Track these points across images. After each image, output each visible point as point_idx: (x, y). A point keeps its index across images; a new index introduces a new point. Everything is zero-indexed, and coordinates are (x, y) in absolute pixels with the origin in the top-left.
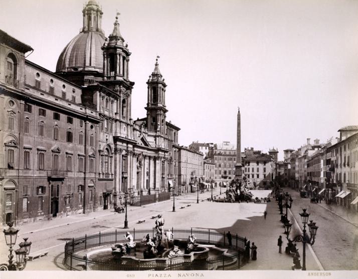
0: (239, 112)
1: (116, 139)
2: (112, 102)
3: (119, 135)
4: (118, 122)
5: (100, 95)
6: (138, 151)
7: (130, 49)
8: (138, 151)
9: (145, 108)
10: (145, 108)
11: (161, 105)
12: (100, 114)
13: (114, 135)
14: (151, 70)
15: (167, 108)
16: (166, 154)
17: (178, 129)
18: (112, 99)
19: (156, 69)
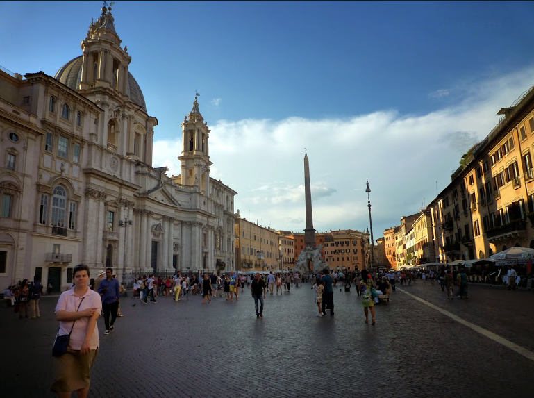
1: (89, 173)
2: (81, 115)
3: (95, 166)
5: (46, 92)
7: (130, 53)
8: (149, 206)
9: (180, 158)
10: (180, 158)
12: (44, 122)
13: (84, 165)
14: (189, 109)
15: (210, 160)
16: (210, 220)
17: (234, 193)
18: (81, 108)
19: (196, 105)
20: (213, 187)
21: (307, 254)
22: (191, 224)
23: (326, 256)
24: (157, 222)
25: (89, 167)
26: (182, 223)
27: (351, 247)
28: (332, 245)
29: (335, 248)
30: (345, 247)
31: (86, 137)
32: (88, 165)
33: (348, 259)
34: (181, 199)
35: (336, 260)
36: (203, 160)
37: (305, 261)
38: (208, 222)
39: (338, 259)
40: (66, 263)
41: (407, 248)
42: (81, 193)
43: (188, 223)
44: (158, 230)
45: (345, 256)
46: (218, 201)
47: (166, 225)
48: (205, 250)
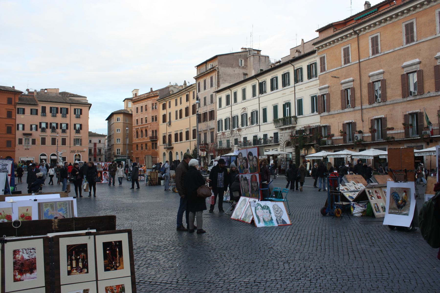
23: (19, 134)
27: (71, 119)
28: (34, 112)
29: (37, 119)
30: (59, 119)
33: (64, 142)
35: (38, 142)
39: (43, 141)
45: (59, 135)
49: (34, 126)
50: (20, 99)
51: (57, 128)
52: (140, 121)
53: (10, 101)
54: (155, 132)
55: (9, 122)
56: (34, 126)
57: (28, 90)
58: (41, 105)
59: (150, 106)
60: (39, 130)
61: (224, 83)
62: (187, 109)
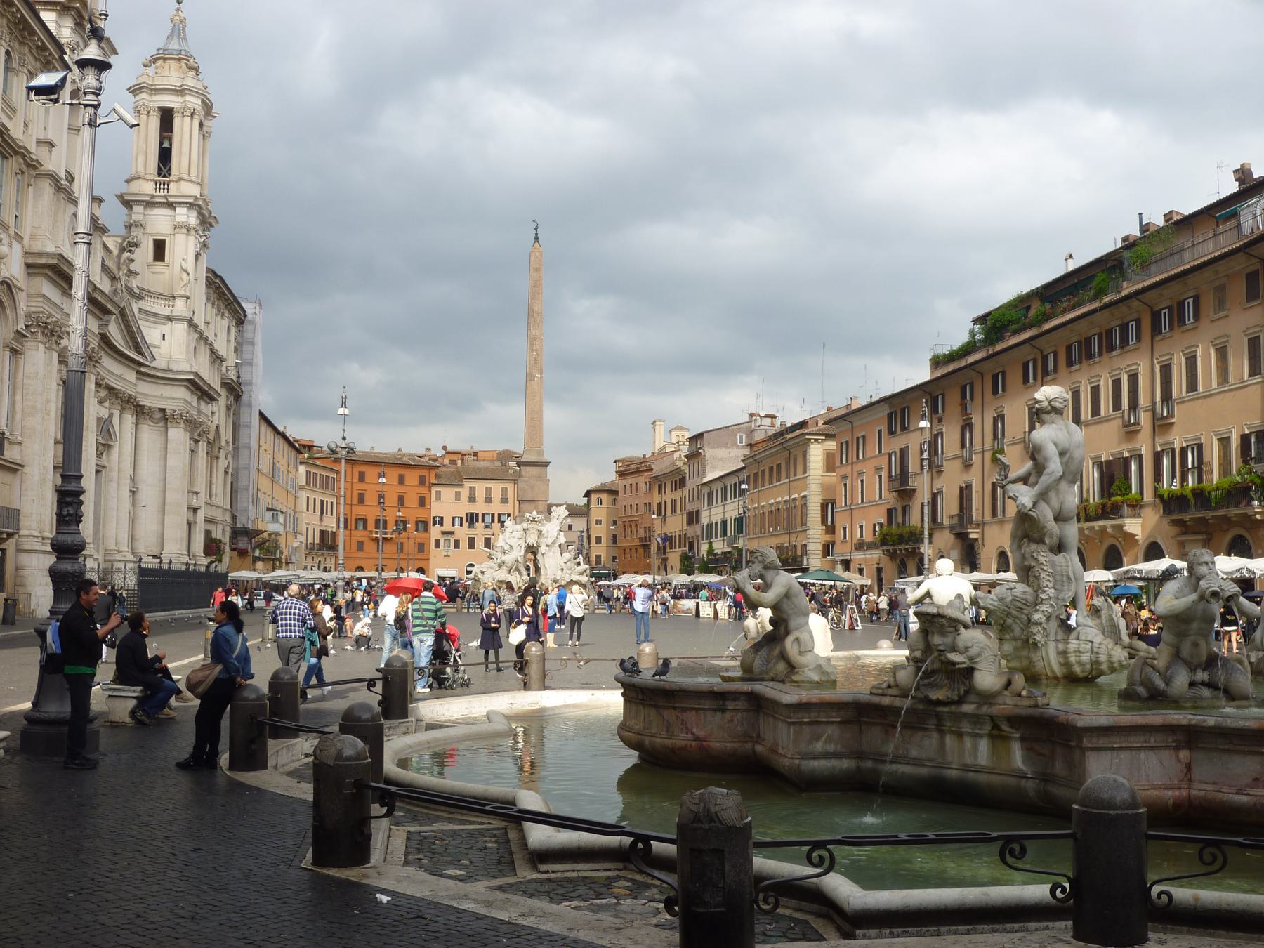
0: (537, 239)
3: (50, 248)
4: (47, 187)
6: (110, 365)
9: (121, 197)
11: (194, 190)
16: (203, 404)
18: (29, 59)
19: (179, 29)
20: (208, 299)
21: (525, 531)
22: (164, 418)
23: (435, 532)
24: (104, 413)
25: (38, 246)
26: (140, 411)
31: (32, 147)
32: (33, 237)
34: (151, 333)
35: (464, 544)
36: (201, 215)
37: (518, 554)
38: (200, 412)
40: (10, 535)
41: (704, 520)
42: (21, 326)
43: (158, 415)
44: (105, 427)
46: (216, 346)
47: (117, 413)
48: (194, 502)
49: (457, 521)
50: (436, 476)
51: (493, 521)
52: (628, 508)
53: (422, 481)
54: (649, 529)
55: (421, 514)
56: (457, 521)
57: (444, 448)
58: (468, 484)
59: (642, 485)
60: (466, 525)
61: (715, 468)
62: (674, 502)
